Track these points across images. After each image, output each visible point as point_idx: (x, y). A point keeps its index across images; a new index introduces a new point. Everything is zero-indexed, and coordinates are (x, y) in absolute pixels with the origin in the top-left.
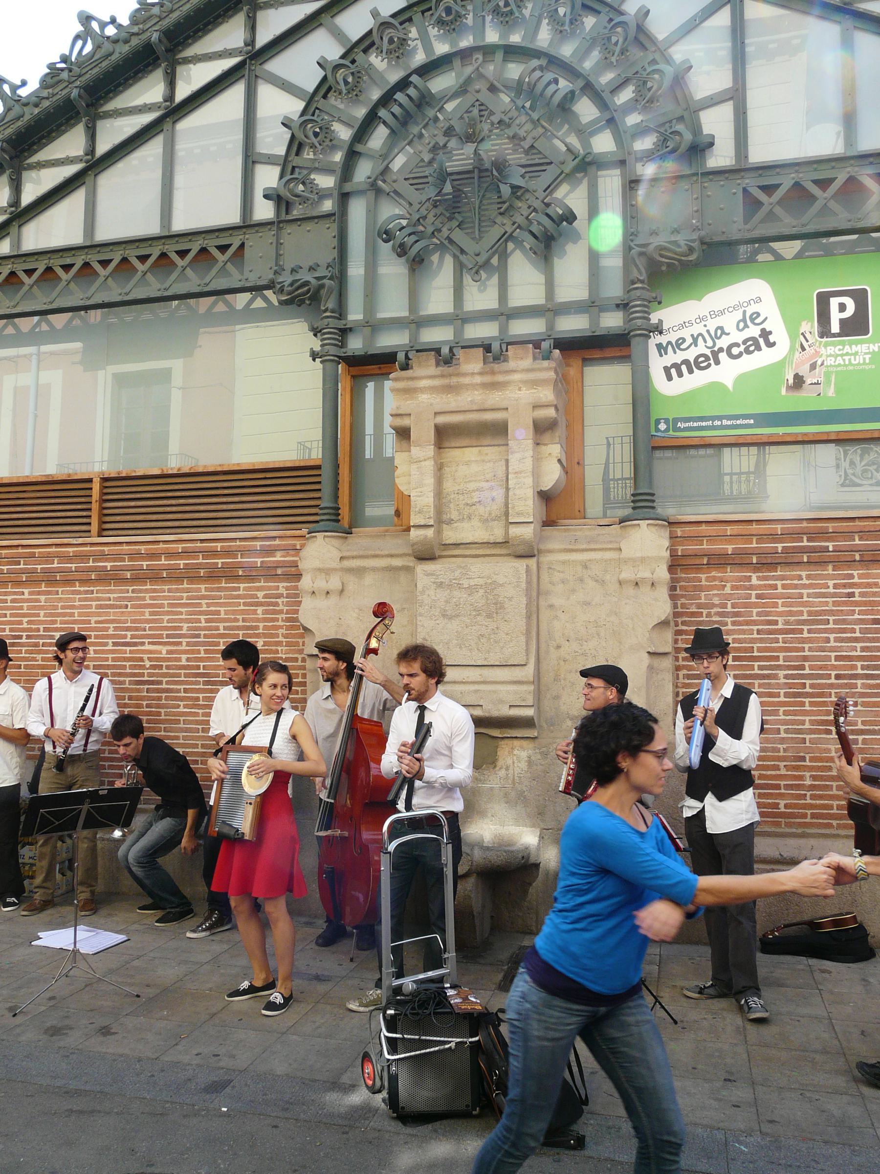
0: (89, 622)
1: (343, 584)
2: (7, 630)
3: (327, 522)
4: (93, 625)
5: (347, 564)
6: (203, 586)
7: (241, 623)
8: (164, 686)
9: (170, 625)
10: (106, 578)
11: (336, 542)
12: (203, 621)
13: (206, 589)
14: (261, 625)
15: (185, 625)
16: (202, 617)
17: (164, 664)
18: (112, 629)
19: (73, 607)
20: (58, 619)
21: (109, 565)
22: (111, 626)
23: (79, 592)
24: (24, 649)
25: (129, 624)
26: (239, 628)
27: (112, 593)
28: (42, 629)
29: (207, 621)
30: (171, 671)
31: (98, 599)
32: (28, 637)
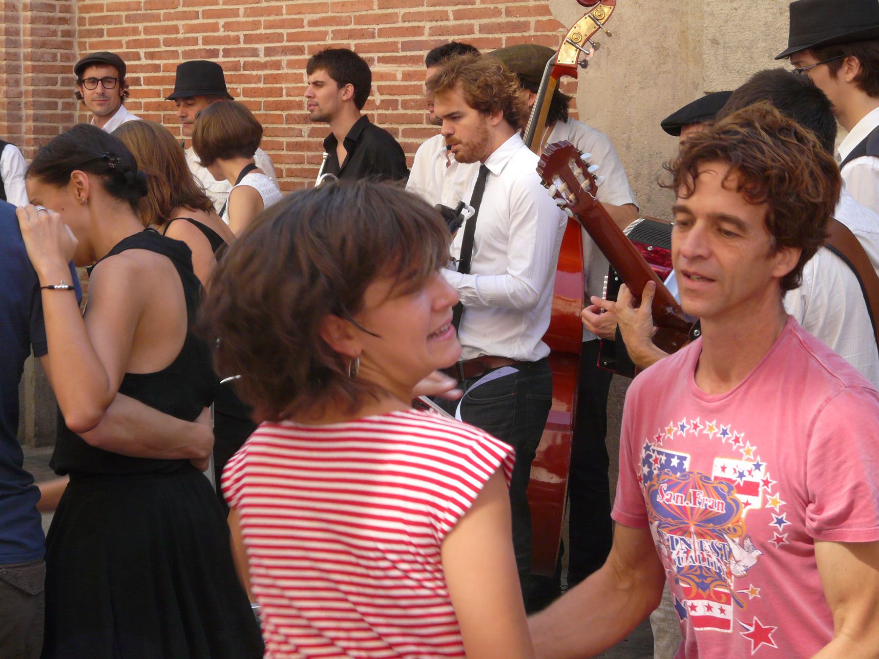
2: (200, 42)
4: (307, 29)
7: (503, 19)
9: (407, 24)
12: (451, 17)
14: (532, 20)
15: (427, 25)
17: (400, 98)
18: (331, 35)
20: (262, 19)
22: (330, 29)
25: (352, 26)
26: (500, 28)
28: (242, 39)
30: (409, 112)
32: (227, 53)
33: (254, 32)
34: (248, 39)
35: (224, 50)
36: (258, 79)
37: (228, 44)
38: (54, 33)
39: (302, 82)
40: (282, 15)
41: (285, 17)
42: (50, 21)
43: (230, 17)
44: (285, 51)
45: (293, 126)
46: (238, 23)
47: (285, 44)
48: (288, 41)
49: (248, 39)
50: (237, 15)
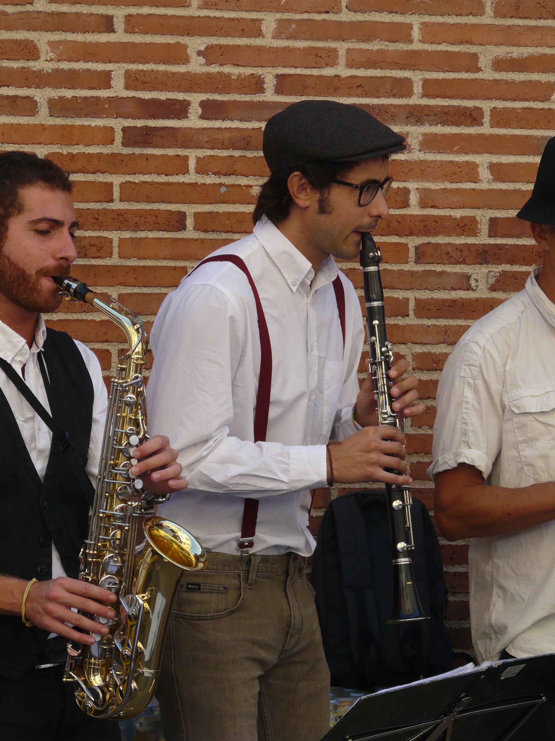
0: (471, 63)
4: (488, 74)
20: (342, 47)
24: (193, 156)
32: (210, 110)
33: (315, 72)
35: (203, 104)
37: (221, 92)
39: (475, 180)
40: (411, 41)
41: (416, 46)
43: (227, 35)
44: (417, 115)
45: (439, 268)
46: (260, 49)
47: (415, 100)
48: (425, 95)
50: (259, 34)
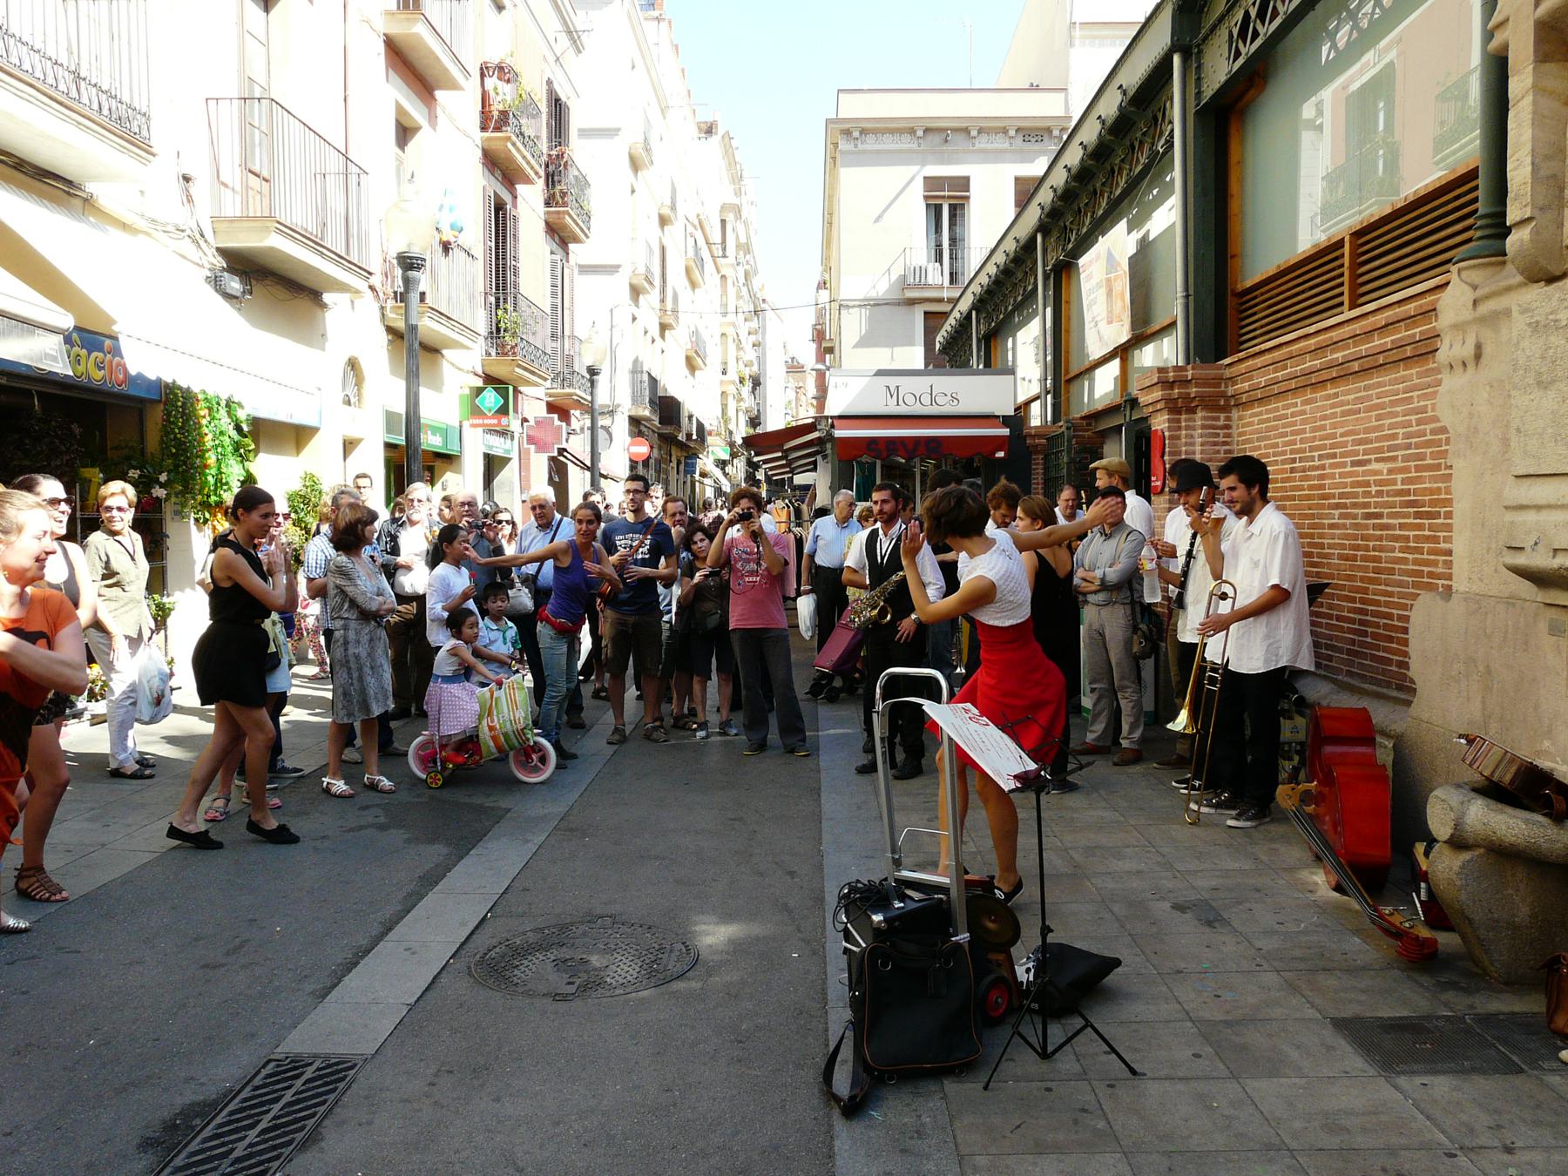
1: (1479, 347)
3: (1485, 242)
5: (1484, 309)
6: (1413, 371)
8: (1385, 521)
10: (1343, 374)
11: (1475, 276)
13: (1420, 375)
15: (1401, 431)
16: (1413, 417)
19: (1324, 418)
21: (1339, 355)
23: (1328, 397)
27: (1349, 393)
29: (1419, 422)
31: (1342, 404)
34: (1312, 449)
36: (1314, 478)
38: (1218, 452)
42: (1215, 444)
49: (1312, 449)
